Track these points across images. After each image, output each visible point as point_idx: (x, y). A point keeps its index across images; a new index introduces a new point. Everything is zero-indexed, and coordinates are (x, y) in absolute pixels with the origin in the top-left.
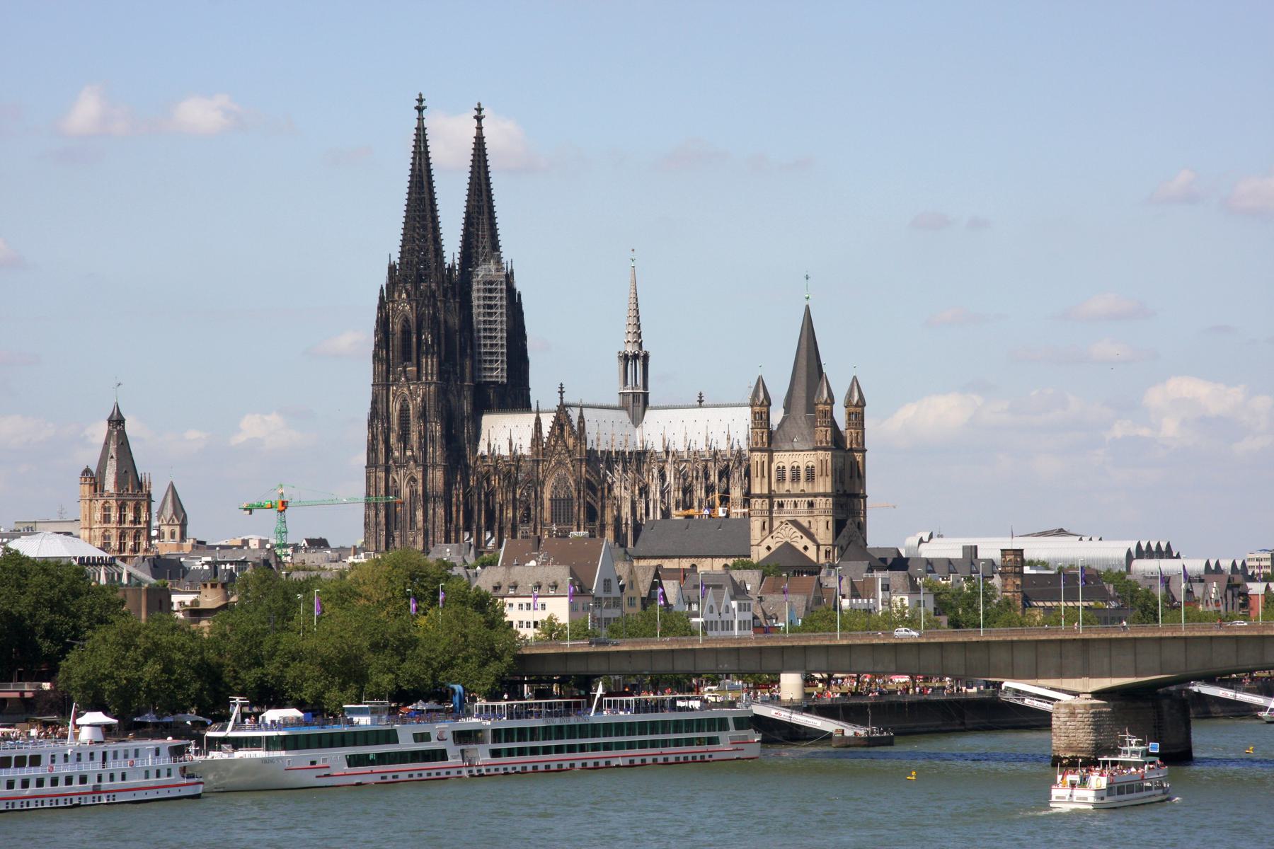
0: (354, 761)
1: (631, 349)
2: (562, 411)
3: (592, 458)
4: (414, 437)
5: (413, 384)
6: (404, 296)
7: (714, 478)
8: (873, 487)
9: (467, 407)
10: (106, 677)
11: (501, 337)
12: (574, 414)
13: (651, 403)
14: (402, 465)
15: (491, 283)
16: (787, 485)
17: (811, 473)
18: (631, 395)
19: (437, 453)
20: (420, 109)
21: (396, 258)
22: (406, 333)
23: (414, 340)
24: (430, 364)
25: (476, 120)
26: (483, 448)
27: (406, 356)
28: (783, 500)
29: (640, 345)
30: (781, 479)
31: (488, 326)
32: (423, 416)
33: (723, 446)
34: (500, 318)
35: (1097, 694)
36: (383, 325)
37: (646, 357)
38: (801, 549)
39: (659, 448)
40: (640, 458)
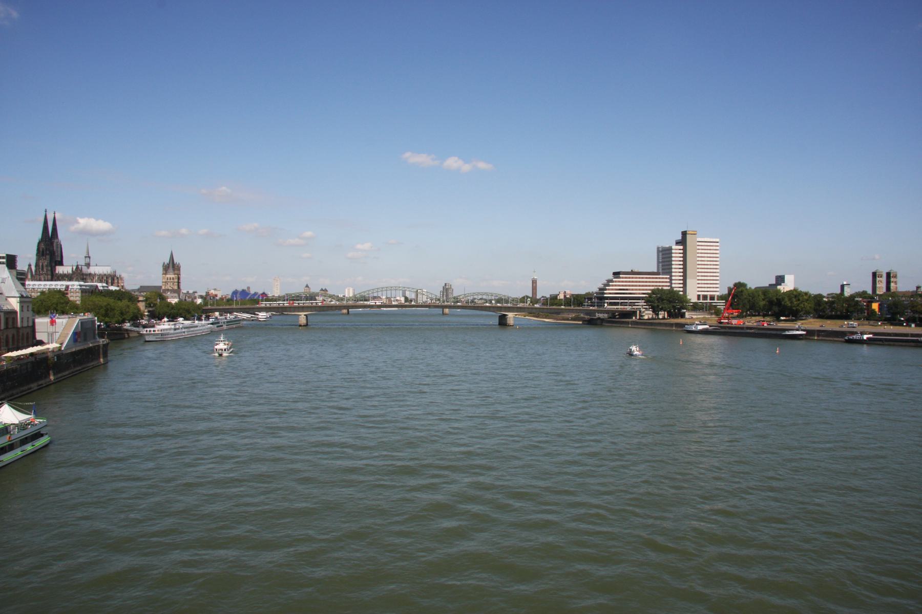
0: (218, 327)
1: (87, 256)
2: (77, 267)
3: (83, 274)
4: (45, 270)
7: (105, 278)
8: (182, 280)
9: (53, 264)
10: (166, 312)
11: (59, 252)
12: (80, 267)
14: (42, 274)
16: (169, 280)
17: (173, 279)
19: (49, 273)
21: (40, 237)
22: (43, 252)
24: (48, 257)
26: (57, 272)
27: (43, 255)
30: (167, 279)
32: (47, 266)
33: (106, 273)
34: (59, 249)
35: (305, 315)
36: (38, 250)
39: (93, 273)
40: (90, 274)
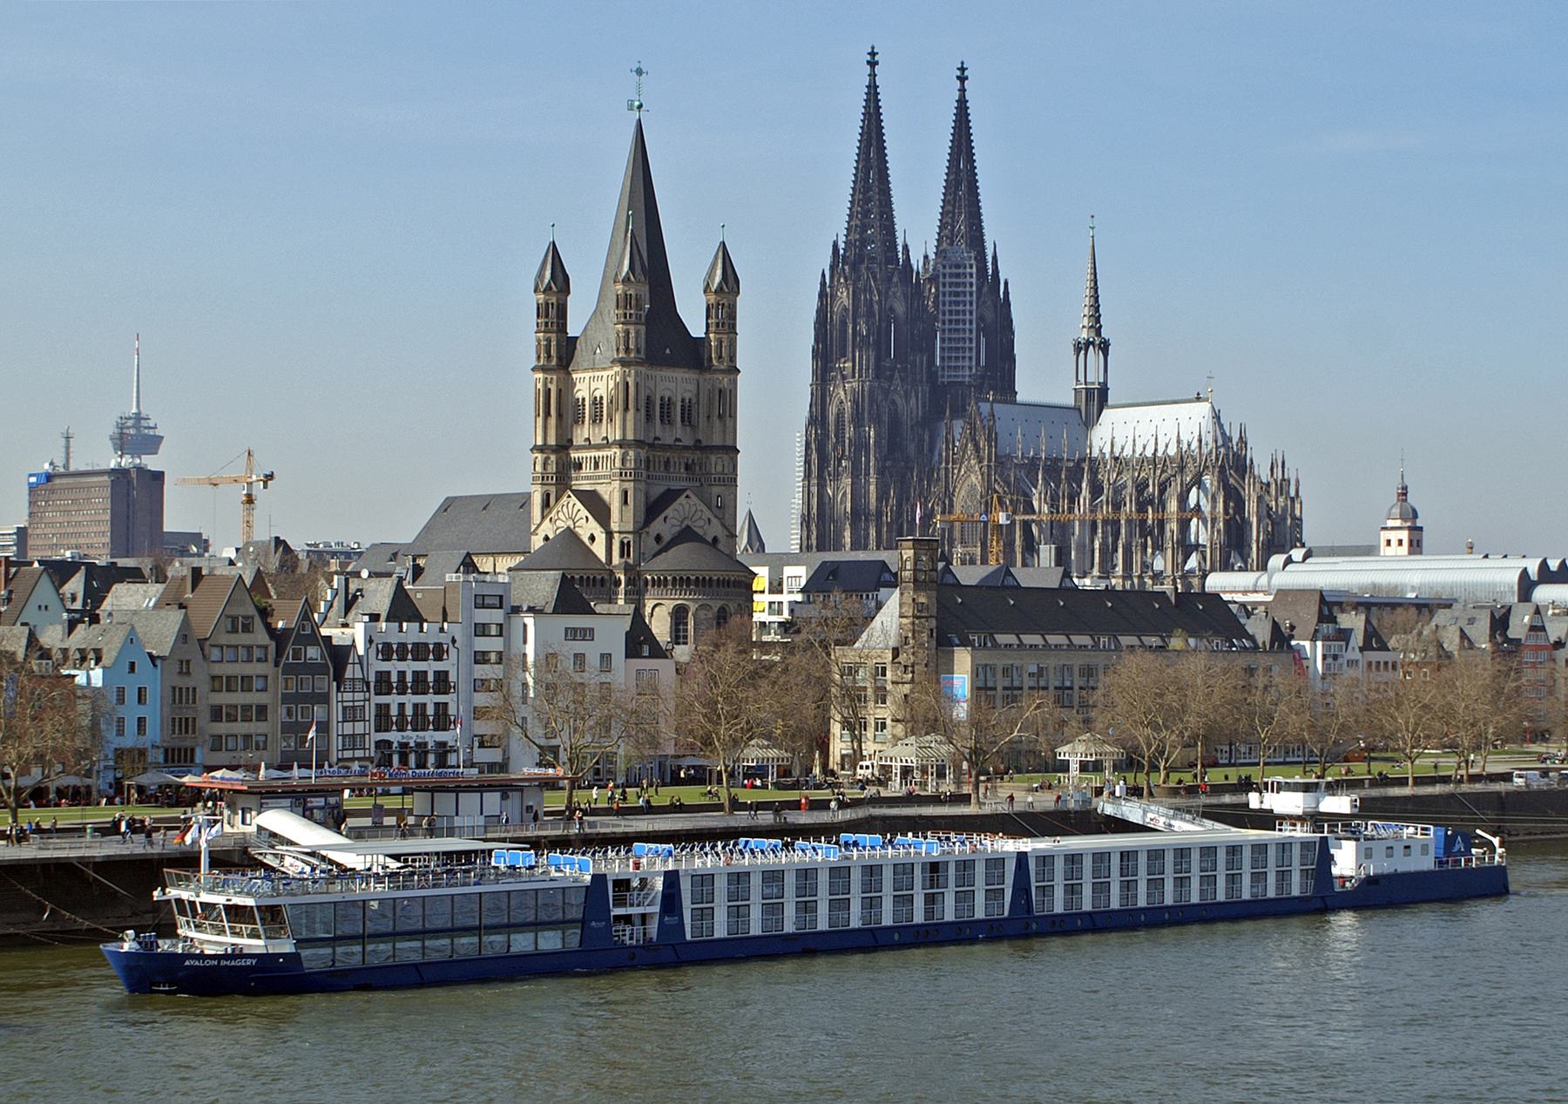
5: (848, 382)
6: (842, 280)
13: (1112, 398)
15: (958, 266)
18: (1084, 391)
20: (873, 64)
23: (850, 331)
25: (958, 82)
28: (580, 455)
29: (1098, 332)
31: (954, 317)
37: (1104, 347)
38: (586, 540)
